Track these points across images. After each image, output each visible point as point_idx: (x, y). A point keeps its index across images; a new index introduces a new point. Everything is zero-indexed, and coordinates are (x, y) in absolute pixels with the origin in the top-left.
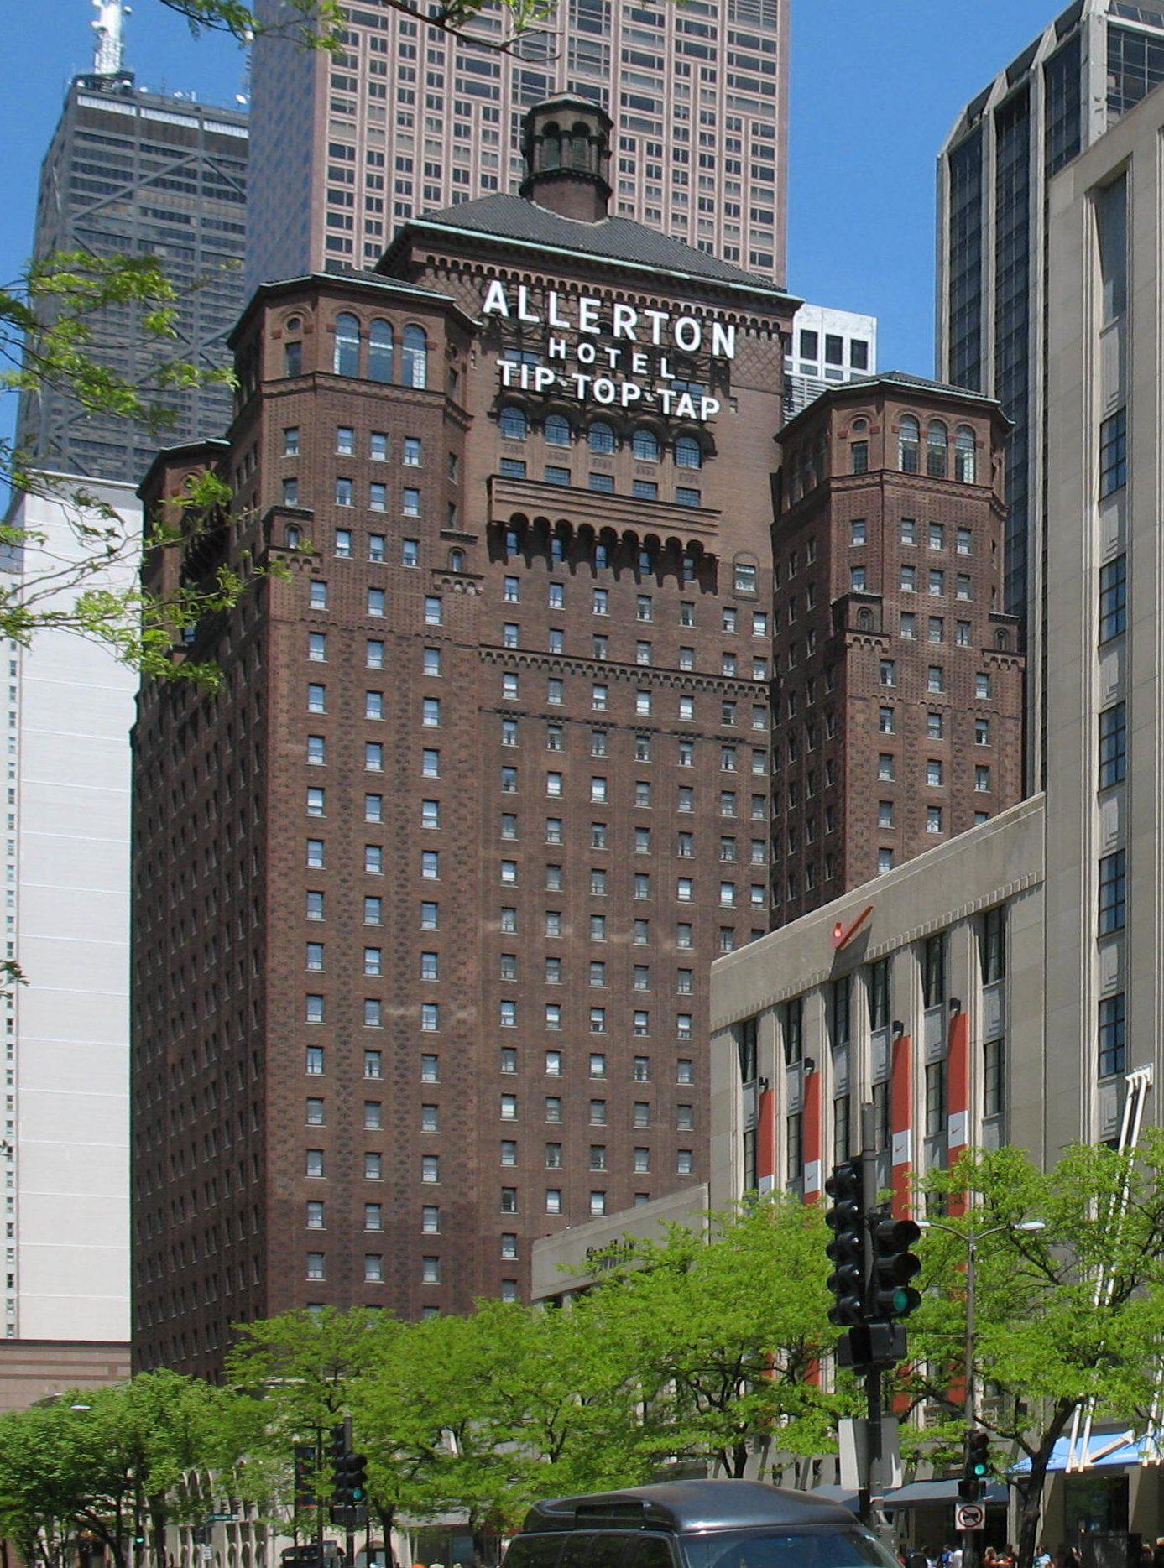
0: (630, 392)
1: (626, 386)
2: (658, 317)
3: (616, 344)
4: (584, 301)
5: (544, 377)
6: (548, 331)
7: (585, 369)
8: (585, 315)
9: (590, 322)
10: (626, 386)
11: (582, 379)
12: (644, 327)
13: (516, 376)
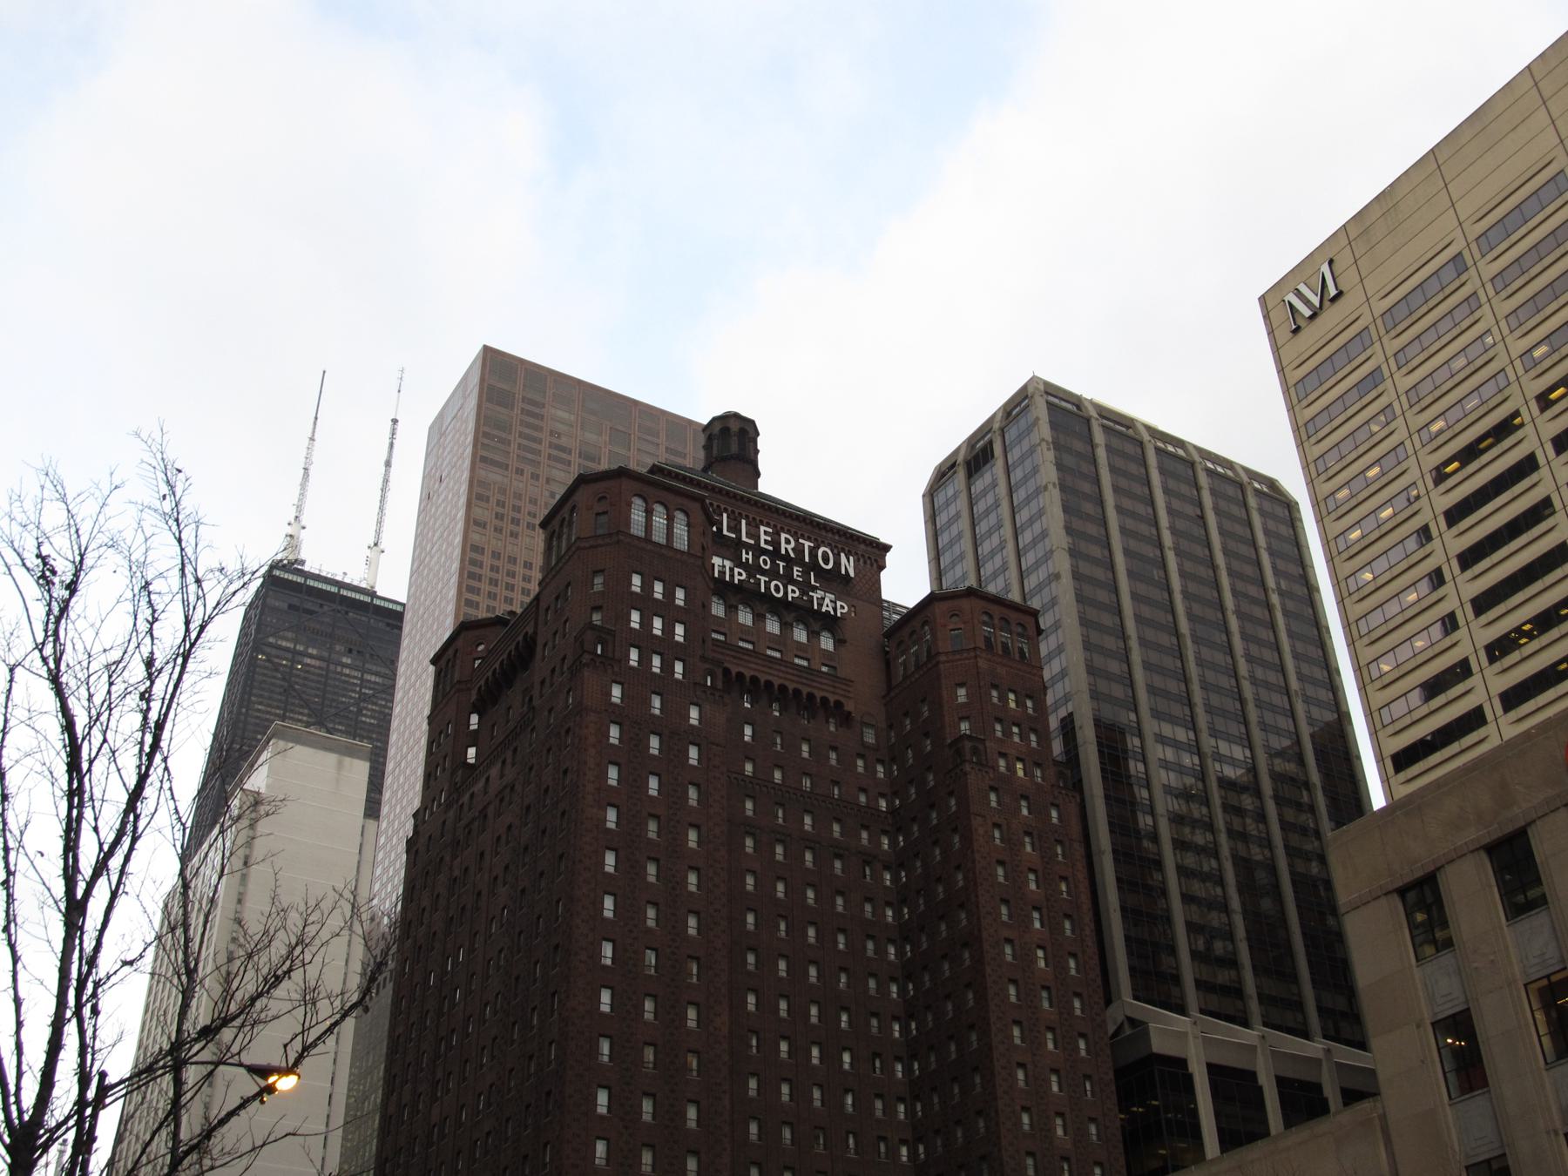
0: (793, 593)
1: (790, 588)
2: (807, 544)
3: (783, 558)
4: (762, 528)
5: (740, 576)
6: (739, 544)
7: (764, 572)
8: (763, 537)
9: (766, 542)
10: (790, 588)
11: (763, 579)
12: (799, 550)
13: (722, 573)
